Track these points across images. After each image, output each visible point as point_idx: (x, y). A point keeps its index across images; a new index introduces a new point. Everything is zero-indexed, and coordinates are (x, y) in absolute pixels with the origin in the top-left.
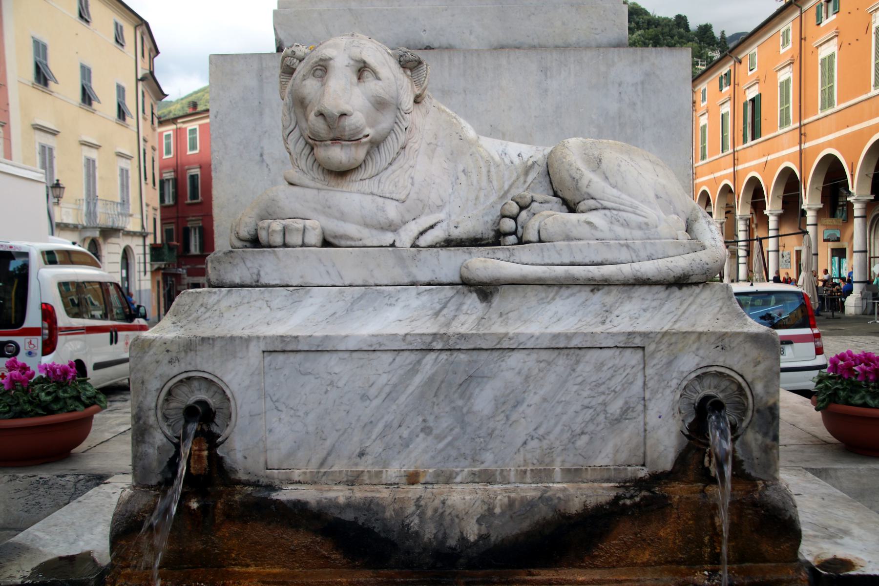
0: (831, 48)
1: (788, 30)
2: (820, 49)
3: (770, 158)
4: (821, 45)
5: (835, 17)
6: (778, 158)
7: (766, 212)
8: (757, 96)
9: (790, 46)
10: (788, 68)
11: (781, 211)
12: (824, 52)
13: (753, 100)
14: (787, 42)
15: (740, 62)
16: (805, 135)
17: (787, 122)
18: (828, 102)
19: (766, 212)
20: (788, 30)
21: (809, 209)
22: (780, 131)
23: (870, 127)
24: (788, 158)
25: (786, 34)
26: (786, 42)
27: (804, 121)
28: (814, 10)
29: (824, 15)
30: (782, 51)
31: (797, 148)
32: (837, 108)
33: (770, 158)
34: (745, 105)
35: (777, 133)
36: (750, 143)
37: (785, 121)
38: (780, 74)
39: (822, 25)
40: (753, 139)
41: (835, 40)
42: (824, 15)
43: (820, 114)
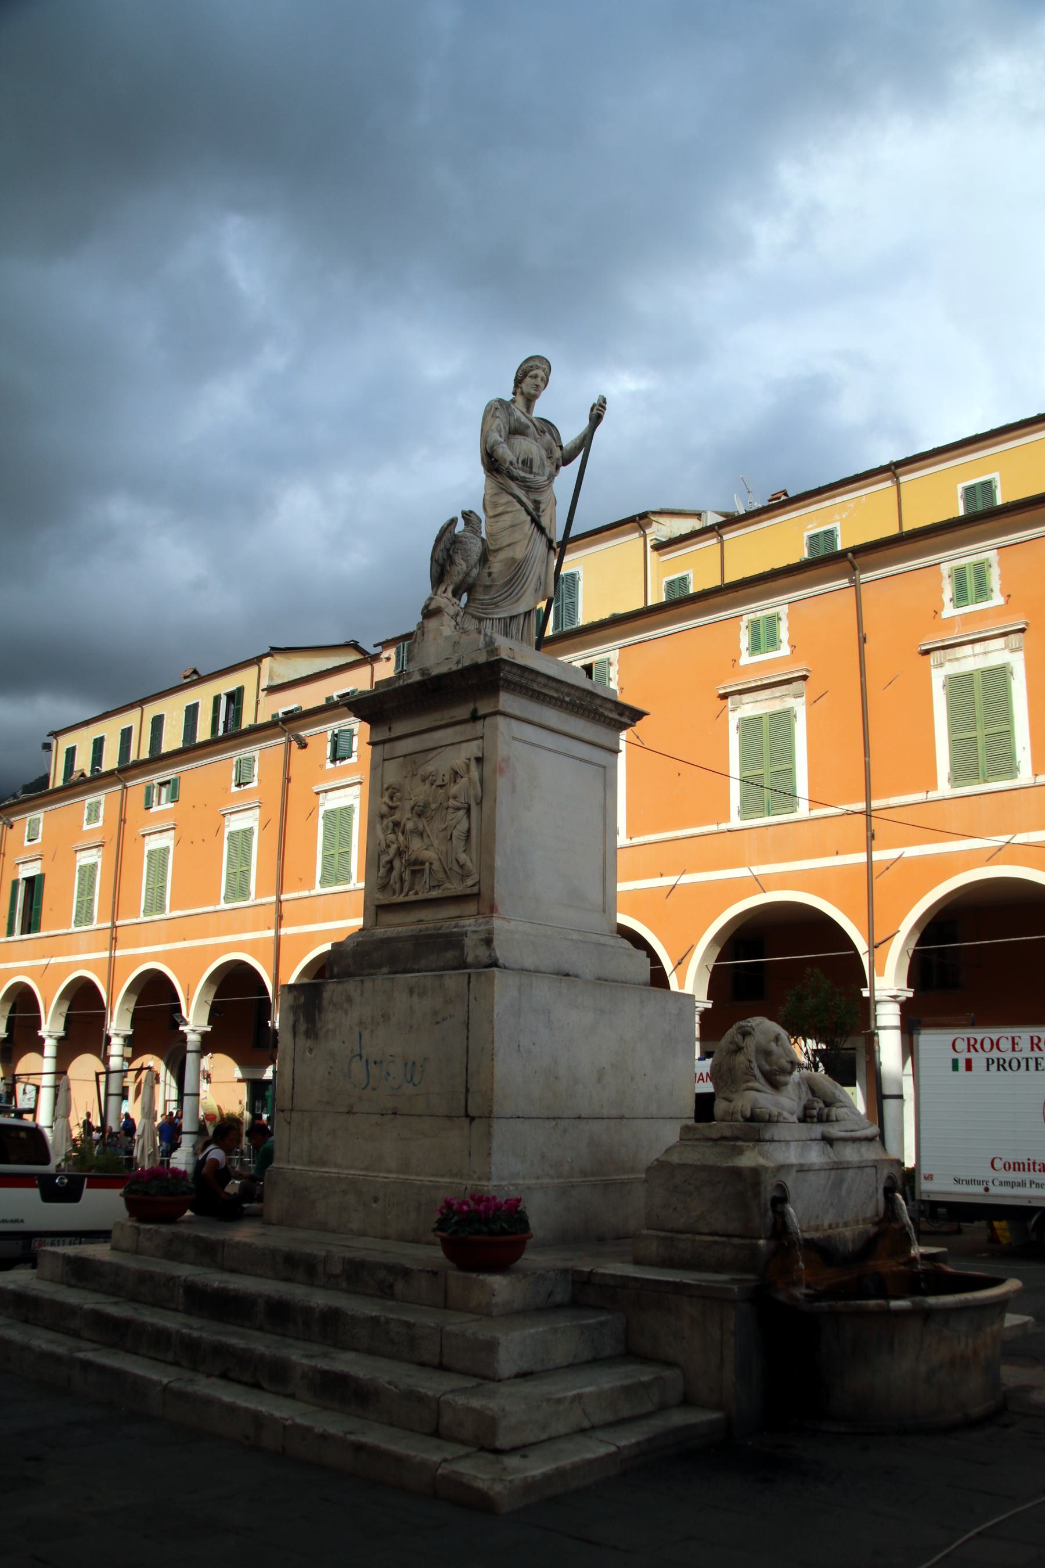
0: (166, 840)
1: (98, 803)
2: (147, 838)
3: (53, 960)
4: (150, 834)
5: (171, 805)
6: (68, 964)
7: (40, 1033)
8: (39, 876)
9: (100, 824)
10: (95, 851)
11: (62, 1034)
12: (153, 843)
13: (30, 881)
14: (97, 818)
15: (11, 827)
16: (116, 939)
17: (89, 919)
18: (156, 904)
19: (40, 1033)
20: (98, 803)
21: (117, 1035)
22: (74, 929)
23: (217, 945)
24: (86, 965)
25: (94, 808)
26: (93, 817)
27: (118, 923)
28: (143, 790)
29: (155, 798)
30: (86, 827)
31: (106, 954)
32: (168, 914)
33: (53, 960)
34: (15, 884)
35: (70, 931)
36: (17, 936)
37: (84, 915)
38: (79, 854)
39: (152, 810)
40: (22, 933)
41: (172, 833)
42: (155, 798)
43: (142, 918)
